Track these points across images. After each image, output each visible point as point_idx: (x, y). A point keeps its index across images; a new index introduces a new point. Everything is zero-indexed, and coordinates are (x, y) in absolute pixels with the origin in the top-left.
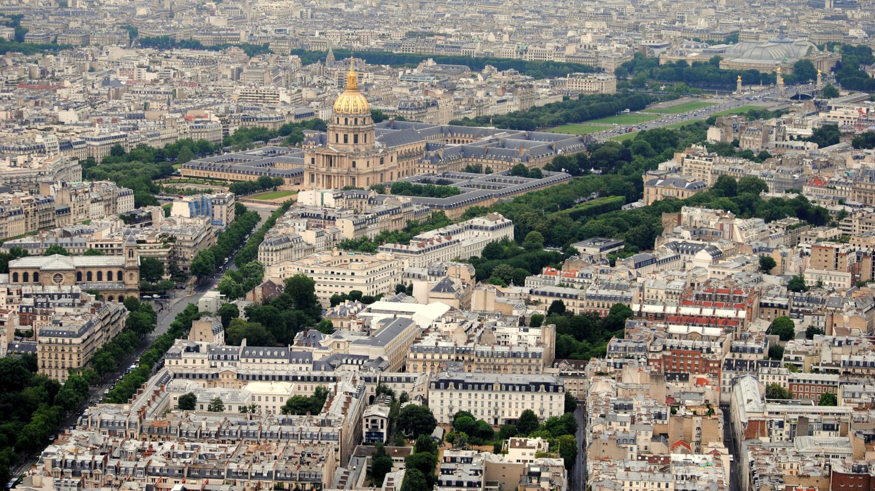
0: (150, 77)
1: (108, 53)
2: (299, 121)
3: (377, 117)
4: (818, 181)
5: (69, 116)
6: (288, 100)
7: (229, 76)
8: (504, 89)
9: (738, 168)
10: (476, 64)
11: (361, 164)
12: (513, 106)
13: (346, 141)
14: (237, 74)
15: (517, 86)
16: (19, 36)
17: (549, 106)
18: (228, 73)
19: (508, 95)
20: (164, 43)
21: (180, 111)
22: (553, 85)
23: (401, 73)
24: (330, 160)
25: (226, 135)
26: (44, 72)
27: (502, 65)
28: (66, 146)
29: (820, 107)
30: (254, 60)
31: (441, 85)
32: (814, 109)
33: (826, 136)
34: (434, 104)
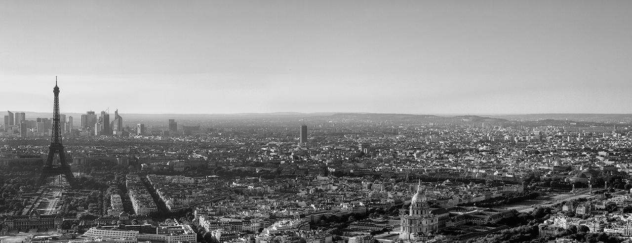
0: (335, 188)
1: (316, 178)
2: (396, 205)
3: (430, 203)
4: (610, 227)
5: (303, 204)
6: (392, 196)
7: (367, 187)
8: (479, 191)
9: (577, 223)
10: (466, 181)
11: (424, 222)
12: (483, 198)
13: (417, 213)
14: (370, 187)
15: (484, 190)
16: (279, 172)
17: (497, 198)
18: (367, 186)
19: (480, 194)
20: (339, 174)
21: (348, 202)
22: (499, 189)
23: (436, 185)
24: (411, 221)
25: (367, 210)
26: (290, 186)
27: (476, 181)
28: (302, 216)
29: (608, 196)
30: (377, 180)
31: (454, 190)
32: (605, 197)
33: (612, 208)
34: (451, 198)
